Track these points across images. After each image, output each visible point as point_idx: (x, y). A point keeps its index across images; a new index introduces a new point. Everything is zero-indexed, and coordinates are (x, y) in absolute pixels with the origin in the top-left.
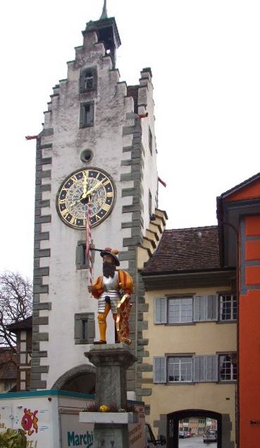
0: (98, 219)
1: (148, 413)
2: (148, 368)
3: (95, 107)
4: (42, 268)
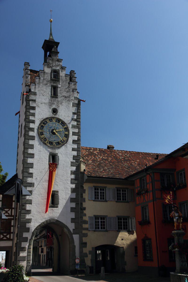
0: (61, 144)
1: (86, 247)
2: (86, 222)
3: (59, 89)
4: (29, 163)
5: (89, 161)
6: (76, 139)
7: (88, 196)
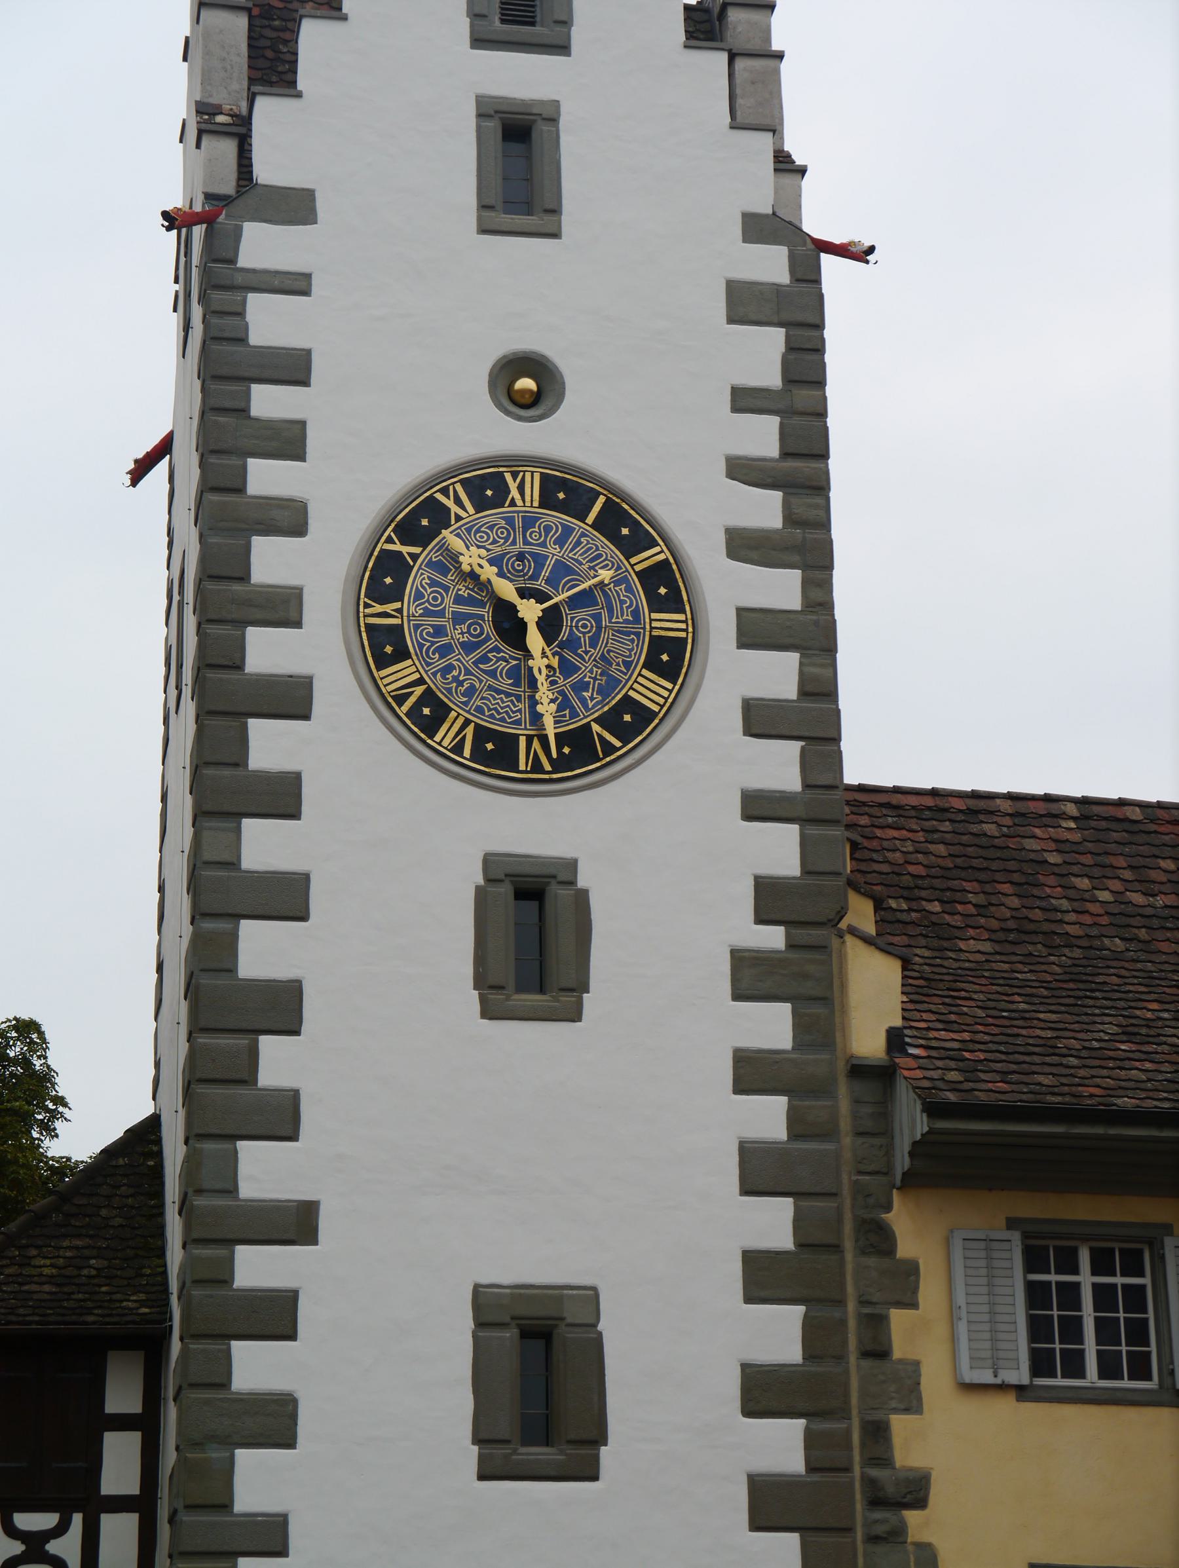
0: (609, 749)
5: (962, 945)
6: (788, 689)
7: (954, 1339)
